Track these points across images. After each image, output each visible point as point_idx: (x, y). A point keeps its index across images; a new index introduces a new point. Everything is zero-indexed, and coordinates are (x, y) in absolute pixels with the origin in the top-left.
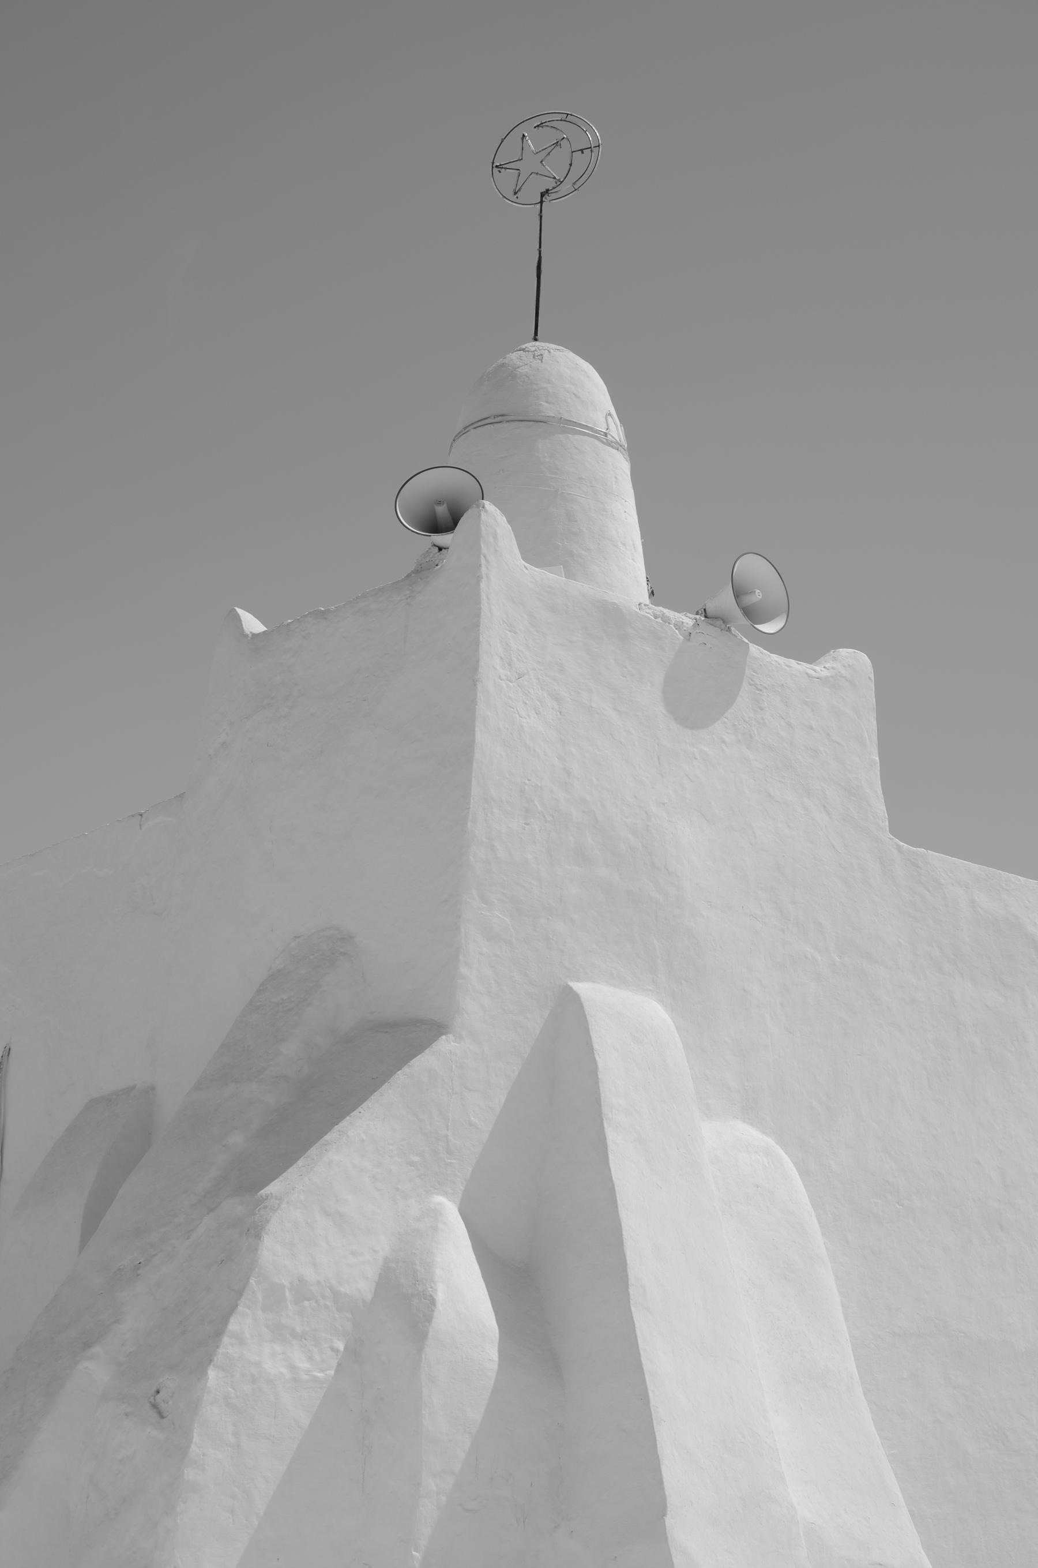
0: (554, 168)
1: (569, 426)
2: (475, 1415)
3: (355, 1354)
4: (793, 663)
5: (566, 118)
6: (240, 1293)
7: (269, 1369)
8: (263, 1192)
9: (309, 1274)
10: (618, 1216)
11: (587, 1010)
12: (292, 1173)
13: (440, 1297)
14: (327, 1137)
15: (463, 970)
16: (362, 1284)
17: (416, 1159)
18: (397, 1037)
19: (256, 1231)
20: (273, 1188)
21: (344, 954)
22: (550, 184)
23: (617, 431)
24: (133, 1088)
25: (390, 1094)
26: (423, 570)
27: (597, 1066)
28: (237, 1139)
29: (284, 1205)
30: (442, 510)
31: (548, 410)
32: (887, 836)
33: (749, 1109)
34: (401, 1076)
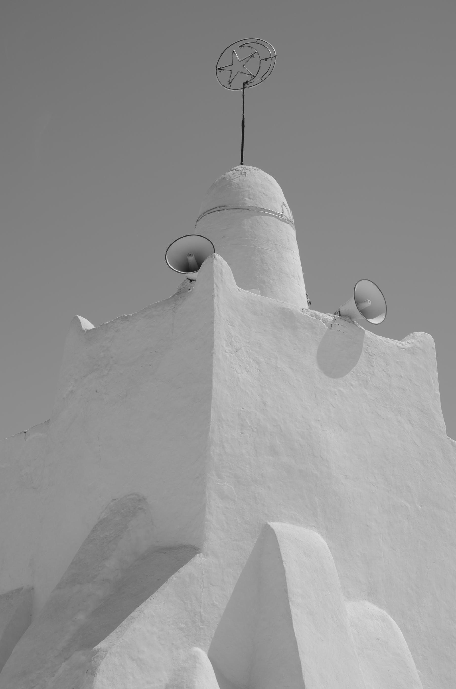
0: (251, 69)
1: (262, 211)
4: (389, 340)
5: (257, 41)
8: (96, 648)
10: (298, 658)
11: (278, 538)
12: (113, 635)
14: (132, 614)
15: (208, 516)
17: (183, 626)
18: (170, 556)
20: (102, 645)
21: (140, 509)
22: (248, 78)
23: (288, 214)
24: (22, 588)
25: (168, 589)
26: (182, 293)
27: (284, 571)
28: (81, 617)
29: (108, 655)
30: (191, 259)
31: (250, 203)
32: (445, 436)
33: (372, 594)
34: (174, 578)
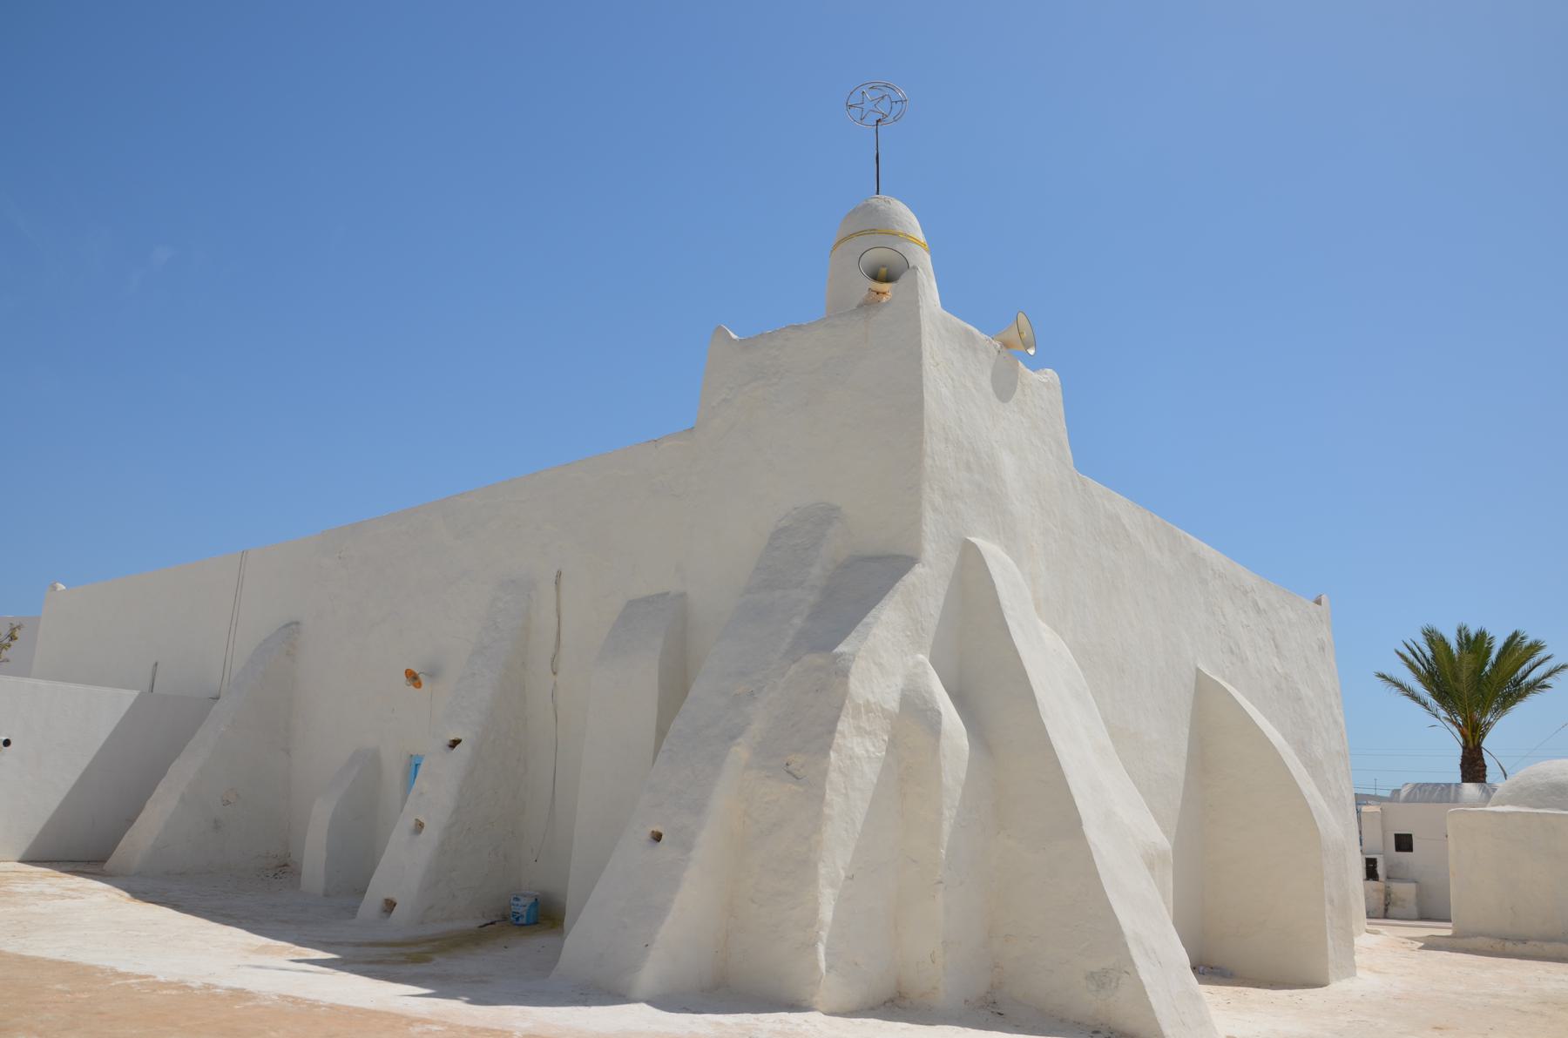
0: (884, 107)
2: (963, 776)
3: (893, 744)
6: (840, 708)
7: (858, 752)
9: (872, 700)
13: (942, 711)
14: (868, 619)
16: (893, 704)
19: (844, 674)
26: (871, 303)
28: (798, 621)
30: (883, 270)
31: (899, 229)
34: (899, 586)
